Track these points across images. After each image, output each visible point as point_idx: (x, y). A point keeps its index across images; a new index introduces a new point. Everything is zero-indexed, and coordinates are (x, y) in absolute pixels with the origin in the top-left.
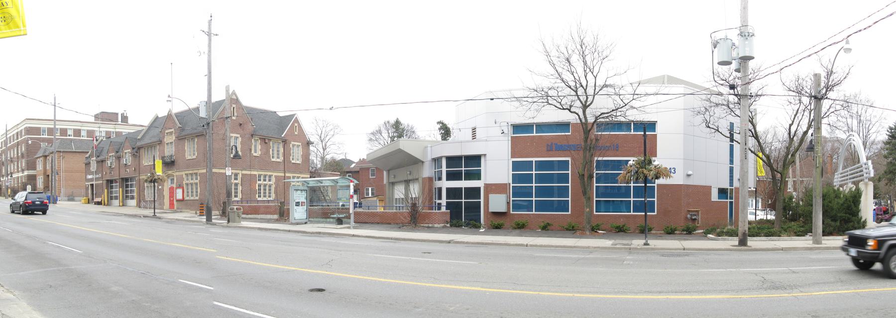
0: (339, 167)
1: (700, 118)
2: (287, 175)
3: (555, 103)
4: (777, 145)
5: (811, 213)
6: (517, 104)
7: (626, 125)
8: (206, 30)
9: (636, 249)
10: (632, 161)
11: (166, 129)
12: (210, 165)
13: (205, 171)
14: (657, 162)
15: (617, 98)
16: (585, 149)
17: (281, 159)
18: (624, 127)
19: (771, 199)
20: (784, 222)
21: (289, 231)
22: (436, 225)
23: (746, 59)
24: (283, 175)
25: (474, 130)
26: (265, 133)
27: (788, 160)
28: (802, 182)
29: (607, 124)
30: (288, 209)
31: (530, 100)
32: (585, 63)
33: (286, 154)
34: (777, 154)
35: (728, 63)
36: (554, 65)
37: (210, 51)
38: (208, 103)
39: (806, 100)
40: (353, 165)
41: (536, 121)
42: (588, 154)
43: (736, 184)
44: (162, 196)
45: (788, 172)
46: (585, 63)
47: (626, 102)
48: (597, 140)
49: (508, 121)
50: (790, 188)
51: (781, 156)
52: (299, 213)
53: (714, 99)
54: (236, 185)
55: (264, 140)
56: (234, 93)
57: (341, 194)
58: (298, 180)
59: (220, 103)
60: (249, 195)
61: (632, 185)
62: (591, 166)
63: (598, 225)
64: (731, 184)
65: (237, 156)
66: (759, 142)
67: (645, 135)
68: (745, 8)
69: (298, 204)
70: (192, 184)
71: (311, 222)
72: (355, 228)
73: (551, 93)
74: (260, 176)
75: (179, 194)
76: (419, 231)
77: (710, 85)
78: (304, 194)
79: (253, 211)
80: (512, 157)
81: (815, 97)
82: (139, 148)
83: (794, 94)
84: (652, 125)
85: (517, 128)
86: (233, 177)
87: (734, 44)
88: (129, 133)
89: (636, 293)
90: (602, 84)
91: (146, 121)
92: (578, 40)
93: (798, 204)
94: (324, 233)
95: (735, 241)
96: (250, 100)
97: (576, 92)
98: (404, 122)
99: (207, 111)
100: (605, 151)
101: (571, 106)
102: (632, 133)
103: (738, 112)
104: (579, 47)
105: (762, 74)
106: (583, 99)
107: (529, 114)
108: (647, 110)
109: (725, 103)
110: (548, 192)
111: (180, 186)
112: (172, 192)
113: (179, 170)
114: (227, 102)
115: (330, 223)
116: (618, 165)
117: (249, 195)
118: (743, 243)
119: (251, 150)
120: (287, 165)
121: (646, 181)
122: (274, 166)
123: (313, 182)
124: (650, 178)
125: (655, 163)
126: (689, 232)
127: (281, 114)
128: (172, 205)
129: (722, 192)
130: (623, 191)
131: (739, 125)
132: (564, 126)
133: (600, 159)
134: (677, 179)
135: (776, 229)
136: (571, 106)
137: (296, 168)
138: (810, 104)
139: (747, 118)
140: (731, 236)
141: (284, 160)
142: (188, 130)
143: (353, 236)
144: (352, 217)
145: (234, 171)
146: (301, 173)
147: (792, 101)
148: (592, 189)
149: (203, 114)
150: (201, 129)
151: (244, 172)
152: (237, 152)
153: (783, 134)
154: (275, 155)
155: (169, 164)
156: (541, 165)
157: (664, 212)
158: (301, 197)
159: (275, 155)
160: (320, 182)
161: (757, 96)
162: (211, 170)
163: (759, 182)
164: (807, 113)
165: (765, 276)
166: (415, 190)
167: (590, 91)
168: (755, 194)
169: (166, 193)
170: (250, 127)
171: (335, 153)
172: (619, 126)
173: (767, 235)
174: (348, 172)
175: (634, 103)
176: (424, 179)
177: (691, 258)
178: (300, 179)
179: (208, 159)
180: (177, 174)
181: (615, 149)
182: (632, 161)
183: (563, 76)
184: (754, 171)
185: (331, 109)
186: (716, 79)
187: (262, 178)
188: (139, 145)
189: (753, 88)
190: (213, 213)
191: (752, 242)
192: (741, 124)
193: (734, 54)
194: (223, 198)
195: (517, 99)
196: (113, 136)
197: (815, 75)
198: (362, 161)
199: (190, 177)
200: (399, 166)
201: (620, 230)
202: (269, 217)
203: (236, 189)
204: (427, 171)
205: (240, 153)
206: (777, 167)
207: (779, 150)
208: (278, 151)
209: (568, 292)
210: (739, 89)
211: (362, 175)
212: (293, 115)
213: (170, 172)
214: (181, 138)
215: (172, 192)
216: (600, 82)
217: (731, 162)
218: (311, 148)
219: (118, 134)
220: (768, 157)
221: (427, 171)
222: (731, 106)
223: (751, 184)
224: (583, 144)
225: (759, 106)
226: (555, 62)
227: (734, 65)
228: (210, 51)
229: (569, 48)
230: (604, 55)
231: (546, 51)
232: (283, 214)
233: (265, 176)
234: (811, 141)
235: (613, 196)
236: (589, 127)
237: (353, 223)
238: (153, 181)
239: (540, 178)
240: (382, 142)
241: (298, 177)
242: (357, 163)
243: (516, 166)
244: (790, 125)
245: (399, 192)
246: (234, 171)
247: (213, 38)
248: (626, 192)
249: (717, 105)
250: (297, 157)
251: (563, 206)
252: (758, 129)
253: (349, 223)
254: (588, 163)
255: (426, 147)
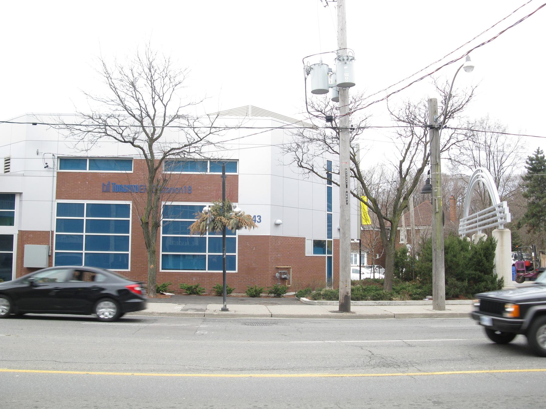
1: (291, 156)
3: (114, 134)
4: (385, 186)
5: (431, 270)
6: (67, 132)
7: (202, 164)
9: (212, 315)
10: (207, 206)
14: (238, 208)
15: (191, 131)
16: (150, 192)
18: (198, 166)
19: (380, 253)
20: (396, 282)
23: (345, 86)
25: (7, 161)
27: (399, 205)
28: (418, 231)
29: (178, 161)
31: (83, 128)
32: (153, 89)
34: (385, 197)
35: (325, 92)
36: (115, 89)
39: (419, 131)
41: (90, 154)
42: (154, 198)
43: (335, 235)
45: (400, 219)
46: (153, 89)
47: (202, 136)
48: (165, 180)
49: (55, 152)
51: (391, 200)
53: (308, 133)
61: (207, 236)
62: (158, 212)
63: (164, 286)
64: (330, 235)
66: (362, 183)
67: (224, 176)
68: (342, 30)
73: (110, 121)
77: (303, 117)
80: (57, 198)
81: (431, 127)
83: (404, 124)
84: (233, 164)
85: (65, 162)
87: (330, 70)
89: (212, 371)
90: (173, 114)
92: (146, 62)
93: (413, 259)
95: (335, 306)
97: (141, 122)
100: (175, 194)
101: (134, 139)
102: (208, 173)
103: (336, 148)
104: (147, 70)
105: (365, 103)
106: (149, 130)
107: (82, 146)
108: (227, 146)
109: (321, 138)
110: (104, 243)
116: (190, 211)
118: (344, 308)
121: (224, 231)
124: (229, 228)
125: (236, 210)
126: (278, 294)
129: (319, 245)
130: (197, 243)
131: (338, 163)
132: (125, 162)
133: (168, 203)
134: (263, 229)
135: (386, 290)
136: (134, 139)
138: (425, 135)
139: (348, 155)
140: (330, 299)
147: (403, 133)
148: (157, 241)
153: (392, 174)
156: (94, 210)
157: (247, 270)
161: (359, 128)
163: (364, 232)
164: (421, 147)
165: (374, 351)
167: (159, 122)
168: (359, 247)
172: (193, 164)
173: (375, 298)
175: (211, 138)
177: (280, 327)
181: (187, 191)
182: (207, 206)
183: (126, 103)
184: (357, 218)
186: (310, 110)
189: (355, 120)
191: (357, 307)
192: (341, 162)
193: (331, 81)
195: (68, 126)
197: (430, 101)
201: (192, 292)
206: (386, 214)
207: (388, 192)
209: (125, 371)
210: (337, 121)
216: (171, 112)
217: (330, 208)
220: (374, 201)
222: (328, 141)
223: (354, 235)
224: (148, 185)
225: (362, 140)
226: (117, 86)
227: (331, 94)
229: (134, 70)
230: (177, 81)
231: (107, 72)
234: (428, 181)
235: (183, 250)
236: (156, 165)
239: (92, 226)
243: (62, 209)
244: (401, 162)
248: (200, 245)
249: (311, 140)
251: (121, 262)
252: (361, 168)
254: (153, 208)
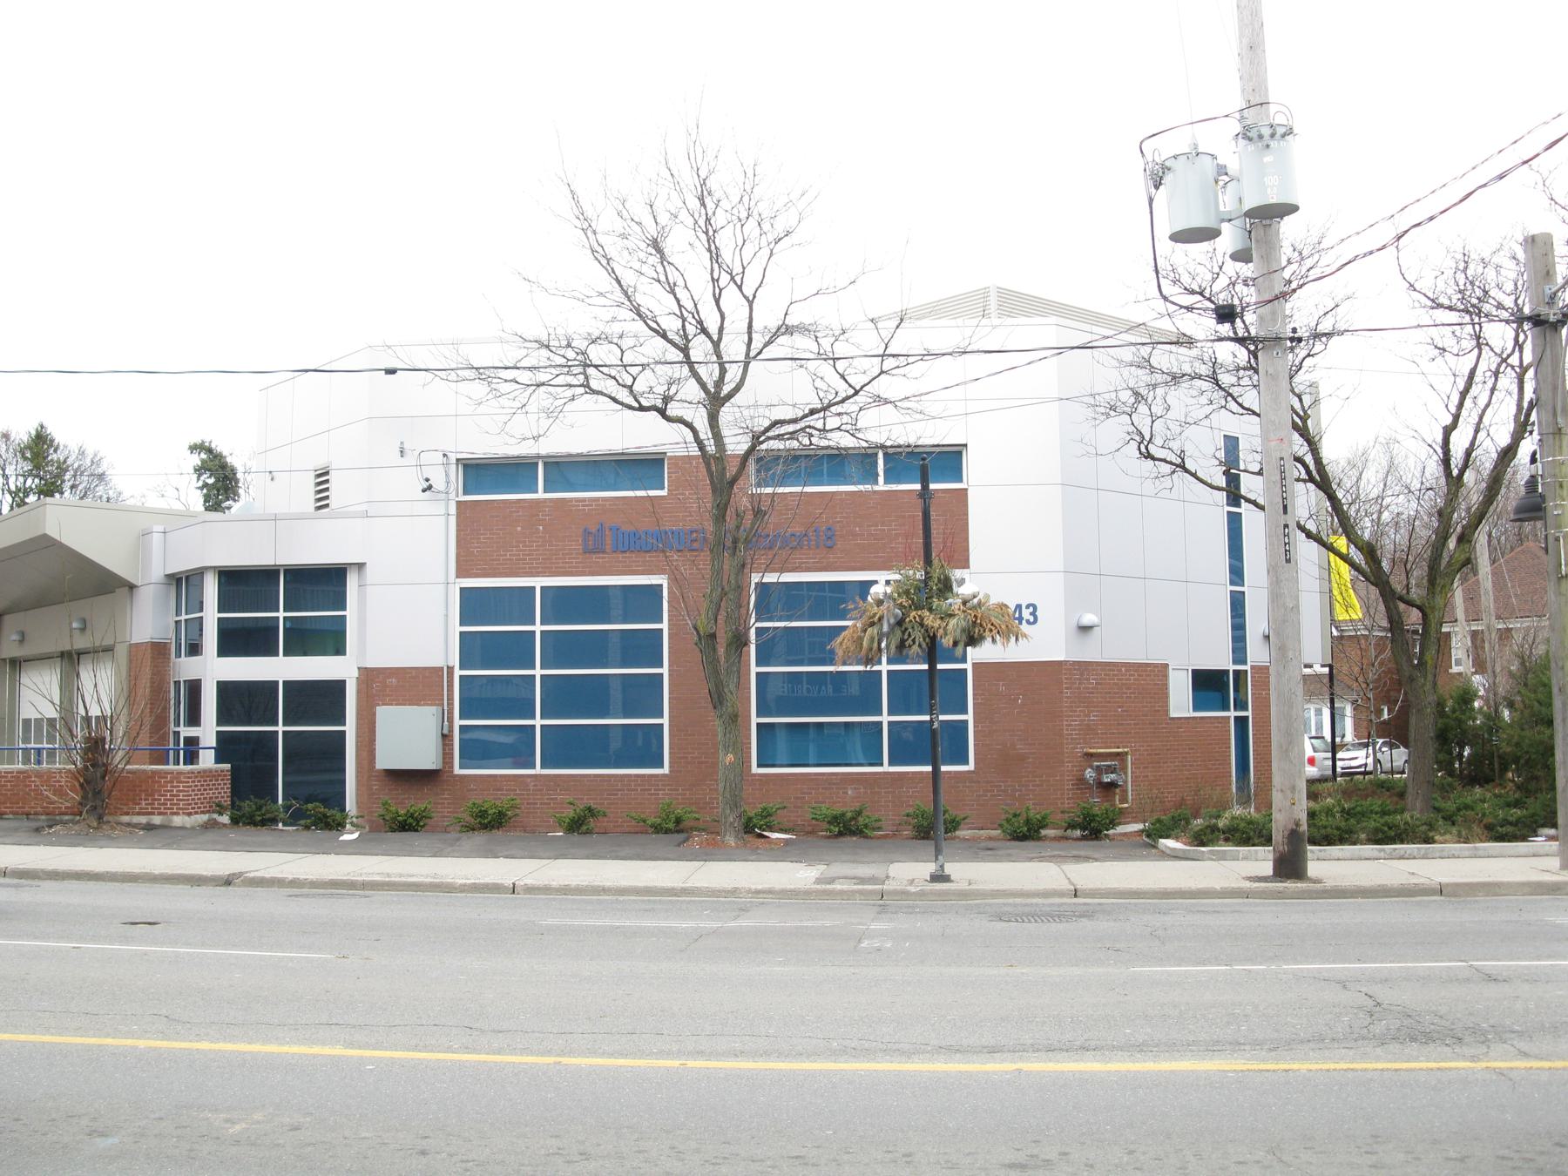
1: (1118, 427)
3: (611, 387)
4: (1401, 505)
5: (1549, 750)
6: (479, 389)
7: (861, 461)
9: (904, 894)
10: (882, 582)
14: (970, 584)
15: (826, 369)
16: (718, 547)
18: (852, 469)
19: (1391, 703)
20: (1445, 790)
22: (178, 820)
23: (1268, 215)
25: (322, 477)
27: (1446, 553)
28: (1506, 634)
29: (794, 457)
31: (525, 377)
32: (715, 256)
34: (1401, 538)
35: (1210, 234)
36: (607, 262)
39: (1500, 335)
41: (547, 447)
42: (728, 564)
43: (1256, 653)
45: (1448, 603)
46: (715, 256)
47: (857, 381)
48: (758, 513)
49: (448, 448)
50: (1460, 661)
51: (1419, 544)
53: (1165, 359)
61: (884, 667)
62: (740, 603)
63: (766, 814)
64: (1239, 653)
66: (1332, 497)
67: (925, 493)
68: (1253, 48)
73: (597, 354)
77: (1148, 311)
80: (461, 573)
81: (1537, 321)
83: (1453, 317)
84: (949, 460)
85: (478, 472)
87: (1222, 170)
89: (908, 1055)
90: (773, 324)
92: (689, 180)
93: (1493, 718)
95: (1261, 861)
97: (685, 350)
98: (68, 438)
100: (789, 550)
101: (667, 399)
102: (881, 486)
103: (1251, 399)
104: (694, 203)
105: (1329, 260)
106: (709, 373)
107: (521, 425)
108: (932, 407)
109: (1204, 370)
110: (590, 696)
116: (834, 599)
118: (1289, 867)
121: (932, 652)
124: (947, 642)
125: (964, 591)
126: (1092, 829)
129: (1208, 684)
130: (854, 690)
131: (1257, 443)
132: (644, 466)
133: (771, 578)
134: (1044, 643)
135: (1414, 813)
136: (667, 399)
138: (1519, 346)
139: (1287, 418)
140: (1247, 841)
147: (1449, 342)
148: (742, 684)
153: (1421, 466)
156: (562, 603)
157: (1000, 761)
161: (1316, 336)
163: (1340, 643)
164: (1507, 381)
165: (1385, 995)
166: (100, 689)
167: (734, 348)
168: (1330, 686)
172: (836, 463)
173: (1379, 838)
175: (884, 386)
176: (134, 649)
177: (1103, 925)
181: (821, 541)
182: (882, 582)
183: (639, 299)
184: (1321, 603)
186: (1168, 289)
189: (1302, 312)
191: (1324, 864)
192: (1265, 438)
193: (1227, 203)
195: (481, 373)
197: (1531, 241)
201: (846, 828)
204: (148, 621)
206: (1408, 586)
207: (1412, 521)
209: (662, 1054)
210: (1250, 317)
216: (767, 318)
217: (1237, 574)
220: (1370, 551)
221: (148, 621)
222: (1226, 379)
223: (1313, 652)
224: (709, 526)
225: (1325, 371)
226: (611, 252)
227: (1229, 239)
229: (658, 205)
230: (780, 229)
231: (582, 215)
234: (1532, 483)
235: (817, 710)
236: (731, 470)
239: (560, 649)
243: (474, 605)
244: (1448, 431)
245: (39, 695)
248: (864, 694)
249: (1176, 378)
251: (643, 748)
252: (1327, 453)
254: (728, 594)
255: (146, 533)
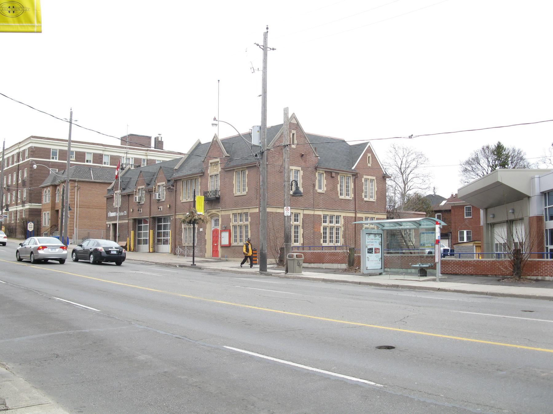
0: (426, 206)
2: (359, 215)
8: (261, 43)
11: (211, 158)
12: (263, 203)
13: (257, 210)
17: (351, 197)
21: (360, 283)
22: (547, 278)
24: (353, 215)
26: (331, 166)
30: (359, 257)
33: (358, 191)
37: (265, 68)
38: (262, 127)
40: (444, 203)
44: (203, 240)
52: (372, 262)
54: (297, 227)
55: (331, 174)
56: (294, 116)
57: (425, 238)
58: (371, 221)
59: (277, 128)
60: (312, 239)
65: (297, 193)
69: (370, 251)
70: (241, 227)
71: (387, 273)
72: (441, 280)
74: (325, 217)
75: (225, 239)
76: (524, 285)
78: (378, 239)
79: (317, 258)
82: (176, 181)
86: (293, 218)
88: (164, 162)
91: (186, 148)
94: (403, 287)
96: (316, 124)
99: (260, 138)
111: (226, 229)
112: (216, 236)
113: (225, 209)
114: (286, 127)
115: (411, 274)
117: (312, 239)
119: (314, 186)
120: (358, 203)
122: (343, 205)
123: (389, 224)
127: (351, 144)
128: (215, 252)
137: (370, 207)
141: (355, 198)
142: (237, 160)
143: (439, 290)
144: (439, 267)
145: (294, 211)
146: (375, 213)
149: (255, 141)
150: (253, 159)
151: (306, 212)
152: (297, 188)
154: (344, 192)
155: (213, 201)
158: (374, 242)
159: (344, 192)
160: (399, 224)
162: (265, 209)
166: (520, 233)
169: (209, 237)
170: (314, 158)
171: (419, 187)
174: (437, 212)
176: (531, 219)
178: (375, 221)
179: (261, 195)
180: (223, 213)
185: (410, 137)
187: (328, 219)
188: (177, 175)
190: (269, 261)
194: (280, 242)
196: (144, 165)
198: (454, 198)
199: (238, 218)
200: (499, 203)
202: (336, 266)
203: (296, 232)
204: (535, 208)
205: (301, 190)
208: (347, 187)
211: (451, 215)
212: (367, 143)
213: (214, 211)
214: (229, 169)
215: (216, 236)
218: (389, 182)
219: (150, 162)
221: (535, 208)
228: (265, 68)
232: (353, 263)
233: (332, 217)
237: (439, 275)
238: (193, 221)
240: (480, 173)
241: (372, 219)
242: (448, 200)
245: (500, 235)
246: (294, 211)
247: (269, 53)
250: (370, 192)
253: (434, 275)
255: (533, 178)
